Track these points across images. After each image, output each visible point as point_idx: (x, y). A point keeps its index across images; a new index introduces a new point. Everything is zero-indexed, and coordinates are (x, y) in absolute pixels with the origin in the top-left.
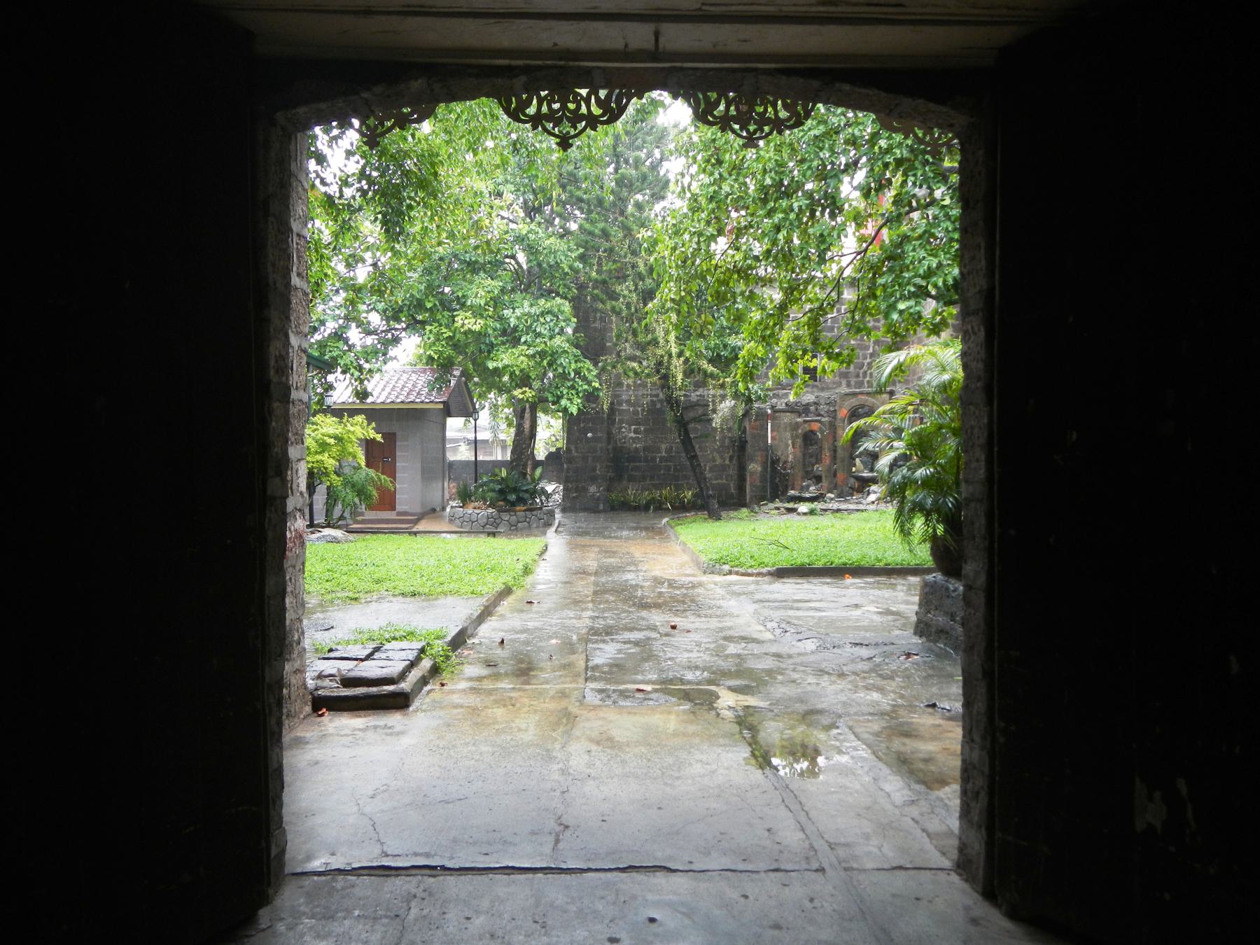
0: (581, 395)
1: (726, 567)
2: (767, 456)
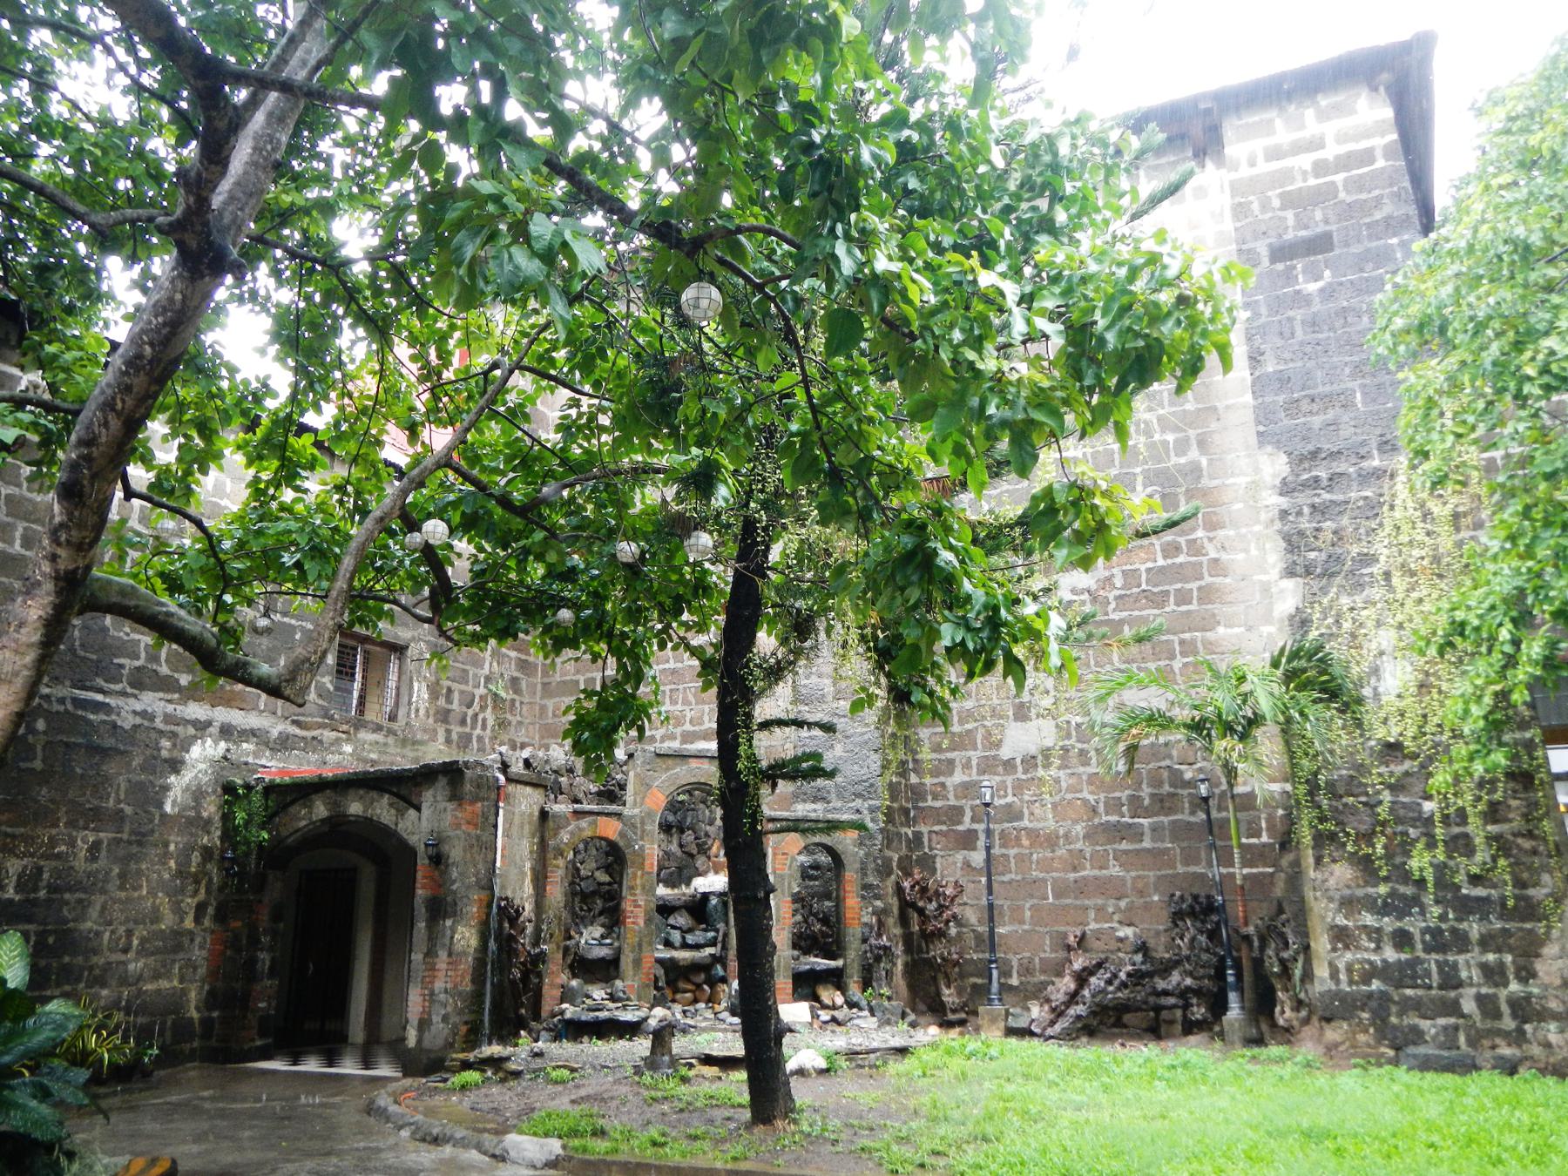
2: (490, 905)
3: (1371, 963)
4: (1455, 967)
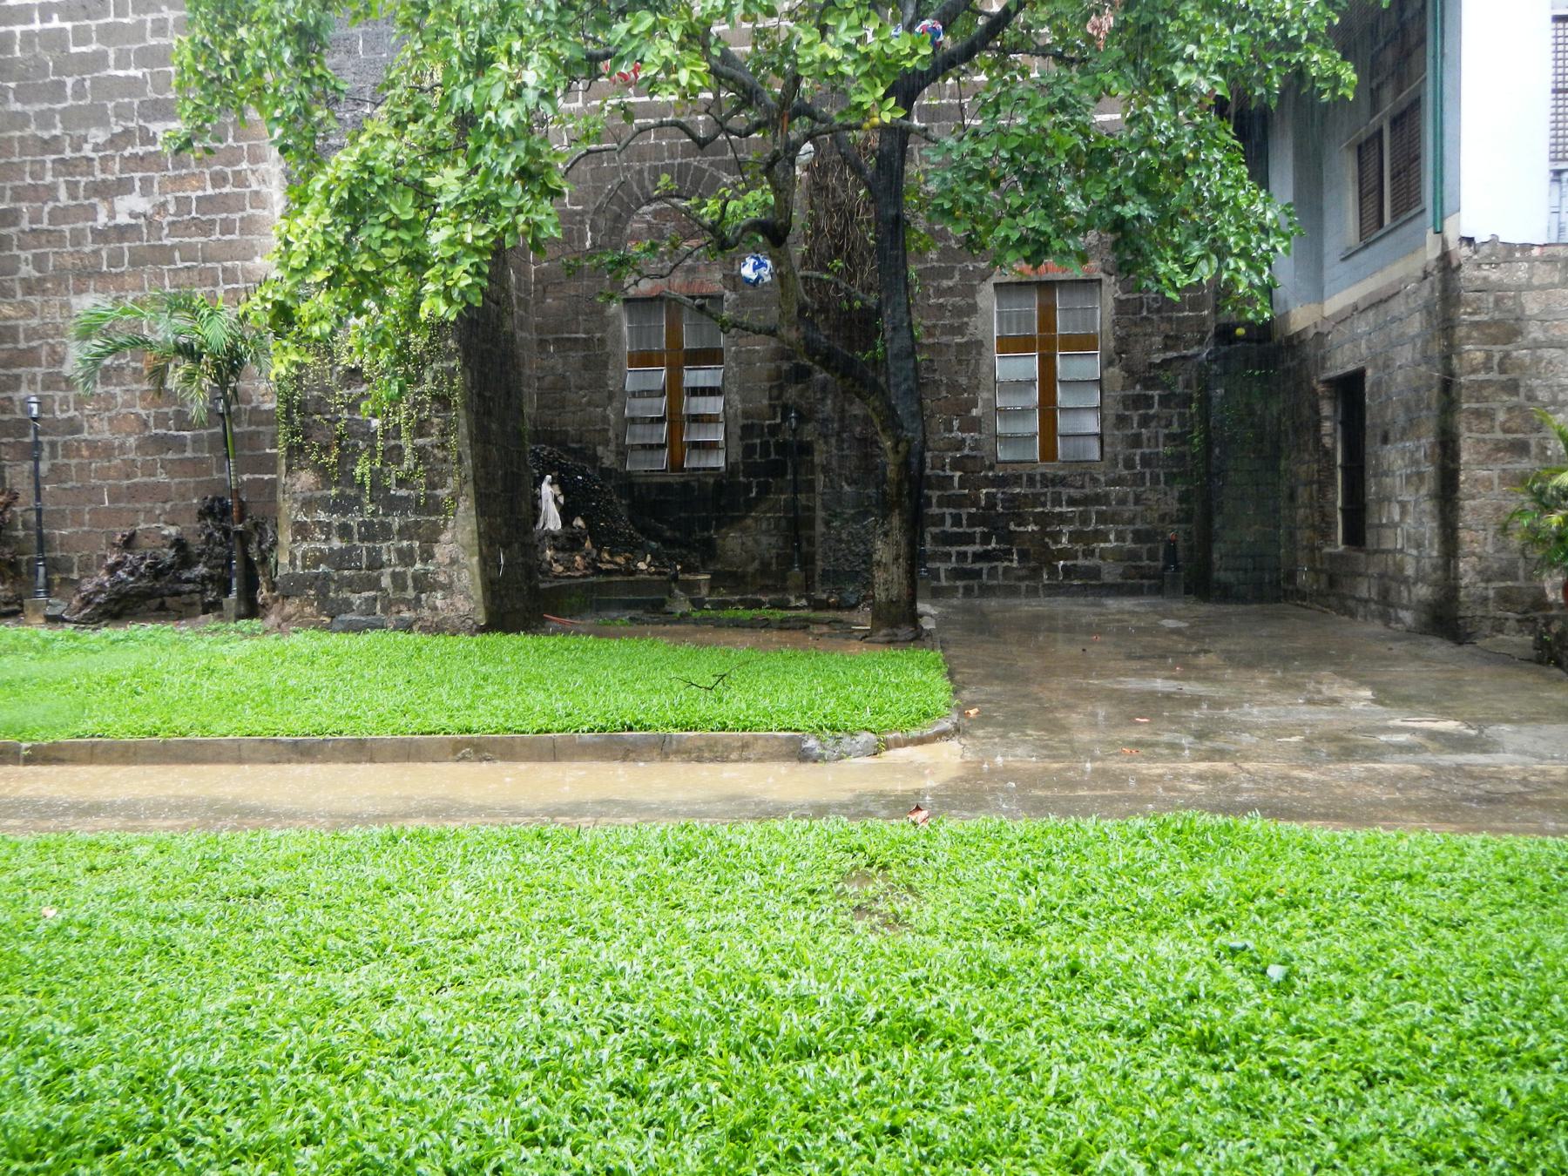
3: (321, 550)
4: (379, 552)
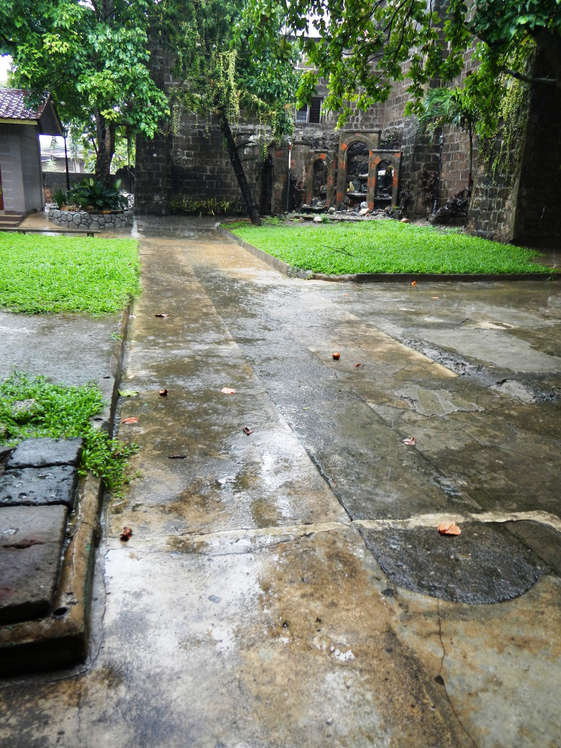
0: (156, 120)
1: (310, 273)
2: (287, 178)
